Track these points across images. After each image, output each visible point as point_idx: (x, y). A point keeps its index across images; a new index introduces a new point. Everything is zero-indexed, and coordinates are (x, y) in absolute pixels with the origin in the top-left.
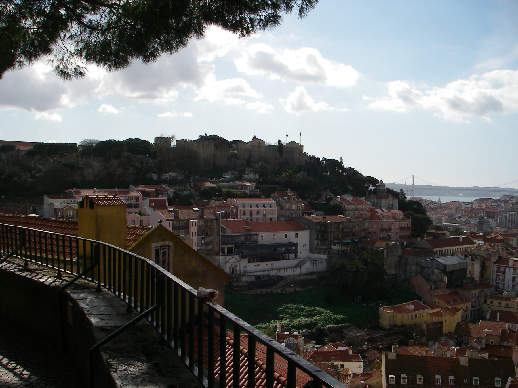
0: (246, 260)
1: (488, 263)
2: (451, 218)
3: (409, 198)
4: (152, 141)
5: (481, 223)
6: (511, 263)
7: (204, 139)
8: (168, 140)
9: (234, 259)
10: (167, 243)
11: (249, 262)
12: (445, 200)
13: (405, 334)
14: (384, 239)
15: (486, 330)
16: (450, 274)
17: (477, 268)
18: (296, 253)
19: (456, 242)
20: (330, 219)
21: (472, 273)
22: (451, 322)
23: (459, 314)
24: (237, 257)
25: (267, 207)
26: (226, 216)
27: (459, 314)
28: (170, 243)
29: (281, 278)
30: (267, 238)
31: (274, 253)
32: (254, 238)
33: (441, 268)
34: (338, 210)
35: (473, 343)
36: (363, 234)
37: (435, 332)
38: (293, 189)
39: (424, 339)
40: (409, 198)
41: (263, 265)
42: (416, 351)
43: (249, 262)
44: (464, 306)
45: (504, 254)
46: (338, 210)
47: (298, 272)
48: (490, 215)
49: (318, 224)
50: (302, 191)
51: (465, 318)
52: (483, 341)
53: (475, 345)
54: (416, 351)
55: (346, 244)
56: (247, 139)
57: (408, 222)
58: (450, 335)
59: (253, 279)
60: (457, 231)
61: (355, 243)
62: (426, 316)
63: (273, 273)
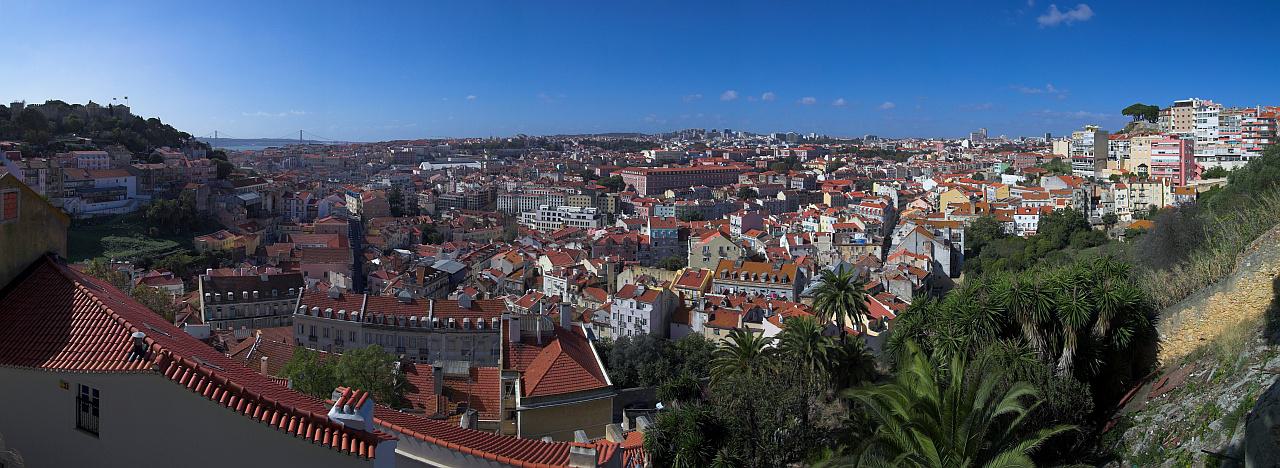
0: (85, 201)
1: (277, 197)
2: (247, 163)
3: (213, 149)
4: (8, 106)
5: (270, 167)
6: (295, 196)
7: (49, 103)
8: (22, 104)
9: (75, 200)
10: (15, 190)
11: (88, 203)
12: (242, 149)
13: (216, 259)
14: (196, 182)
15: (277, 250)
16: (248, 208)
17: (269, 201)
18: (125, 195)
19: (252, 182)
20: (152, 166)
21: (265, 206)
22: (251, 245)
23: (258, 238)
24: (77, 199)
25: (100, 156)
26: (68, 165)
27: (258, 238)
28: (18, 190)
29: (114, 216)
30: (101, 182)
31: (106, 195)
32: (91, 183)
33: (242, 203)
34: (159, 159)
35: (269, 262)
36: (179, 178)
37: (237, 257)
38: (122, 143)
39: (231, 262)
40: (213, 149)
41: (99, 205)
42: (226, 272)
43: (88, 203)
44: (261, 232)
45: (290, 190)
46: (159, 159)
47: (127, 210)
48: (277, 160)
49: (143, 170)
50: (131, 146)
51: (262, 241)
52: (278, 260)
53: (272, 264)
54: (226, 272)
55: (165, 187)
56: (85, 103)
57: (214, 169)
58: (251, 257)
59: (91, 217)
60: (253, 173)
61: (173, 185)
62: (230, 242)
63: (107, 212)
